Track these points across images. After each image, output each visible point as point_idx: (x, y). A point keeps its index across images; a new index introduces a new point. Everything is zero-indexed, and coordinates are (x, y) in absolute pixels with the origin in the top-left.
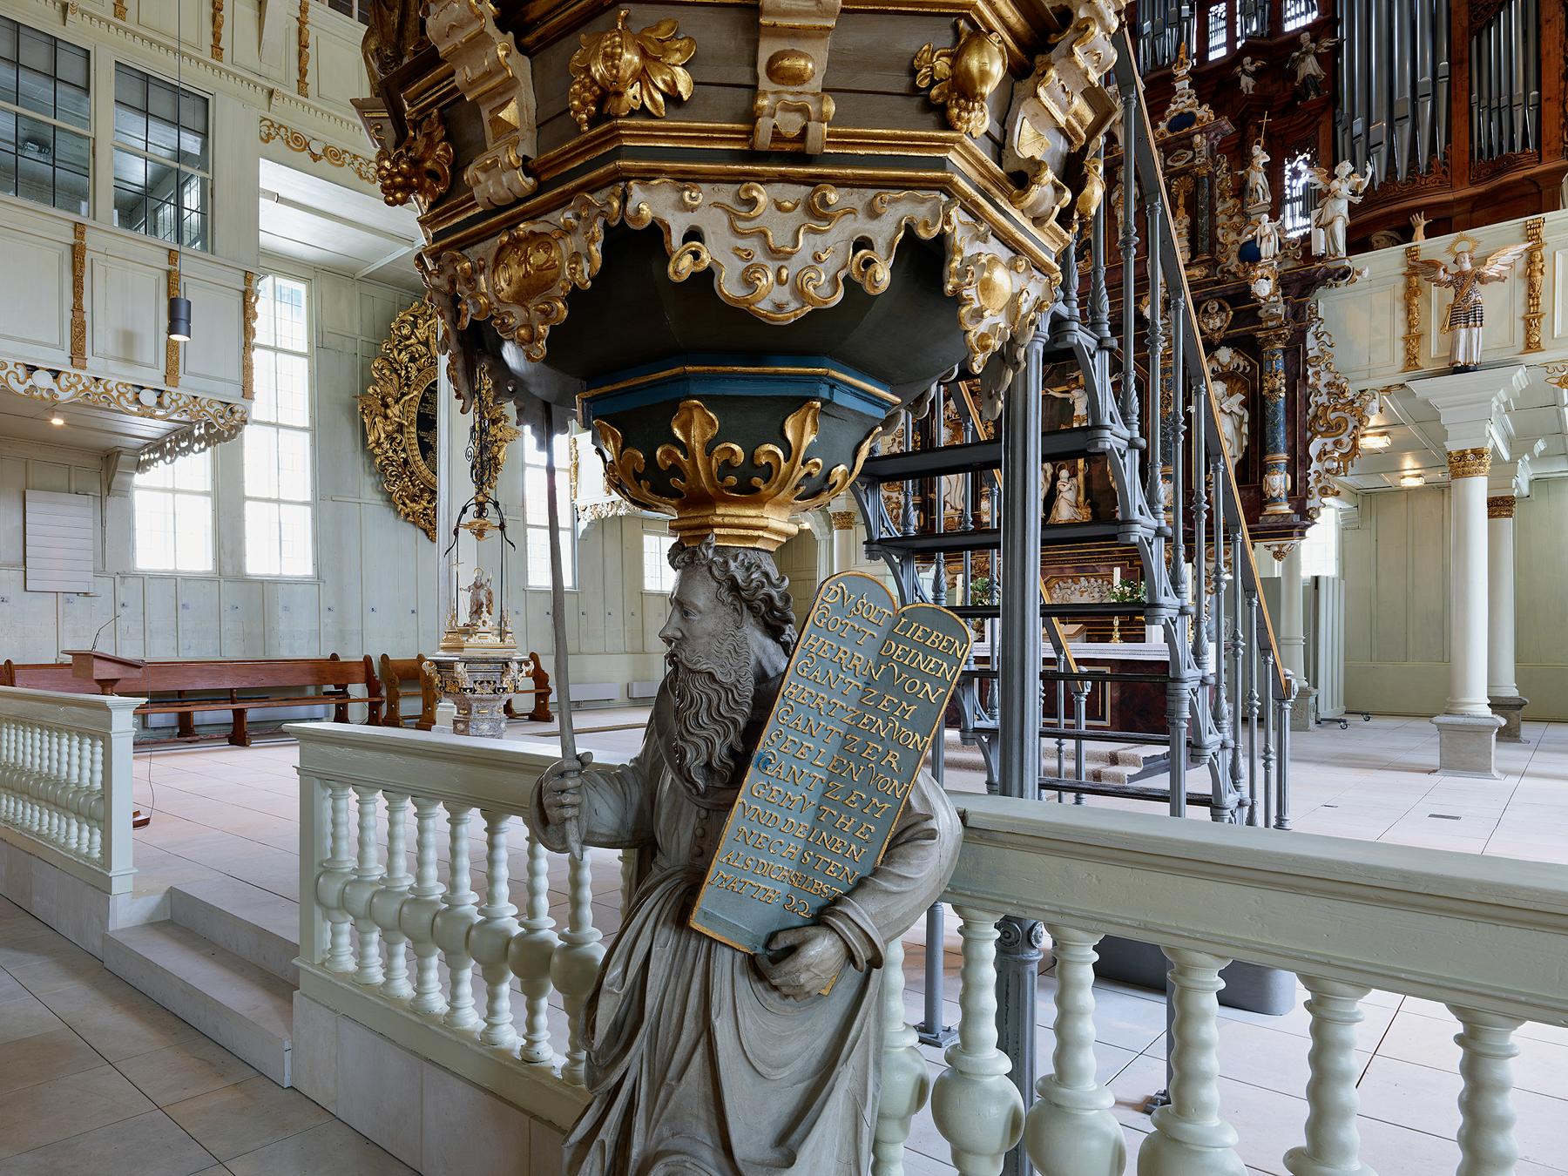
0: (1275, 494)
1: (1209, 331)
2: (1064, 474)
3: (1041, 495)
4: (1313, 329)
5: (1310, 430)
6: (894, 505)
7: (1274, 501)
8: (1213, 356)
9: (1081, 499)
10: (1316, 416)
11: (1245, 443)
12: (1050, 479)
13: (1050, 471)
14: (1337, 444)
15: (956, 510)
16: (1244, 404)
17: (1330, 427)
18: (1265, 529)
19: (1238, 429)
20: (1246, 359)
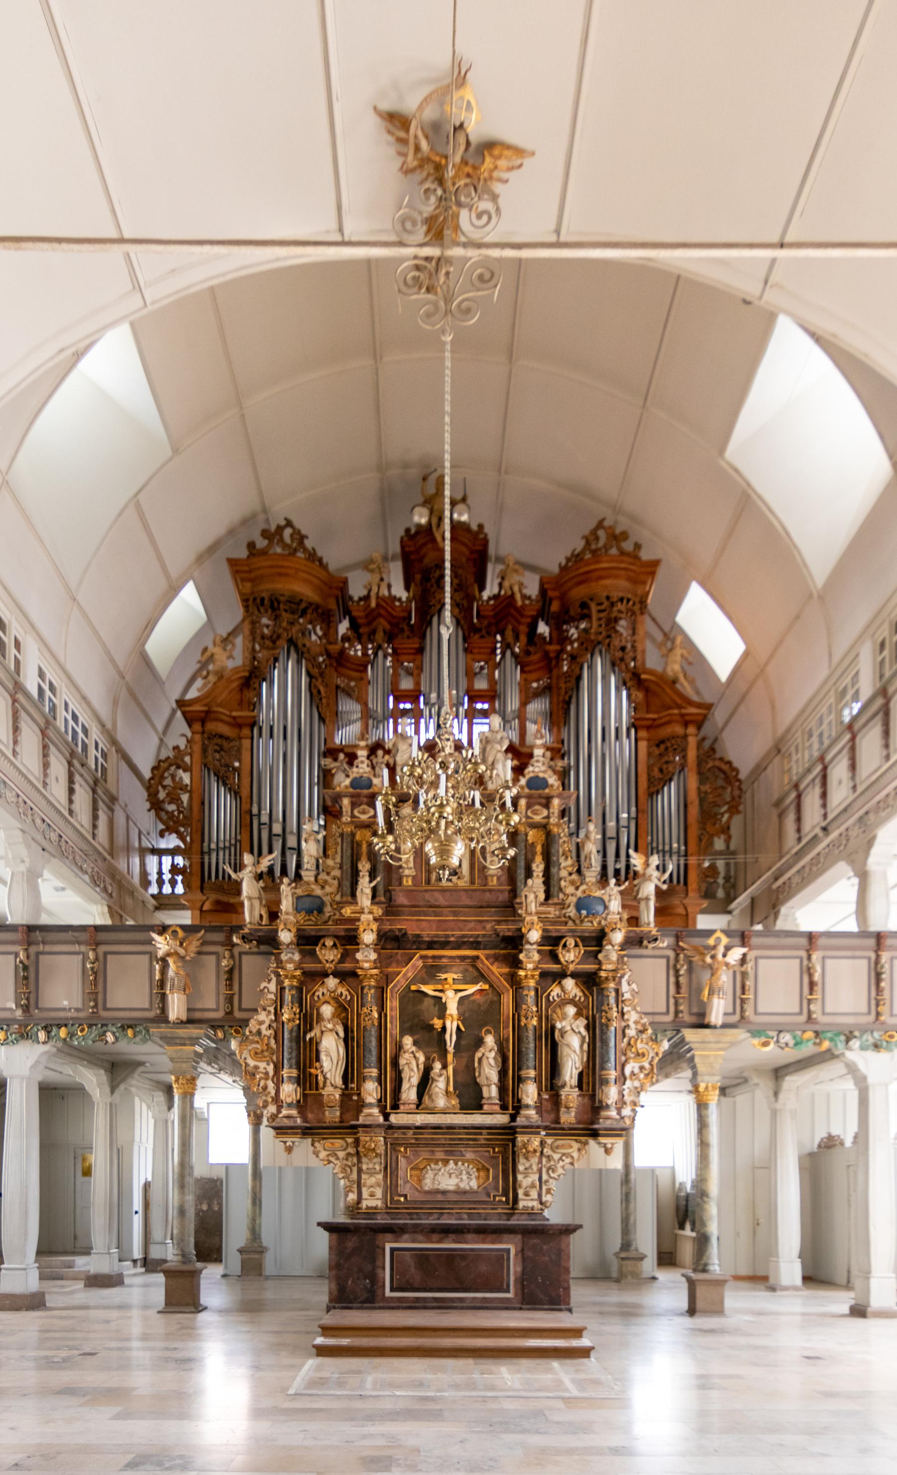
0: (609, 1102)
1: (565, 963)
2: (438, 1066)
3: (415, 1081)
4: (626, 977)
5: (625, 1055)
6: (262, 1075)
7: (607, 1107)
8: (560, 983)
9: (451, 1089)
10: (629, 1044)
11: (585, 1059)
12: (422, 1067)
13: (422, 1058)
14: (642, 1068)
15: (336, 1087)
16: (587, 1027)
17: (638, 1054)
18: (606, 1129)
19: (581, 1046)
20: (582, 991)
